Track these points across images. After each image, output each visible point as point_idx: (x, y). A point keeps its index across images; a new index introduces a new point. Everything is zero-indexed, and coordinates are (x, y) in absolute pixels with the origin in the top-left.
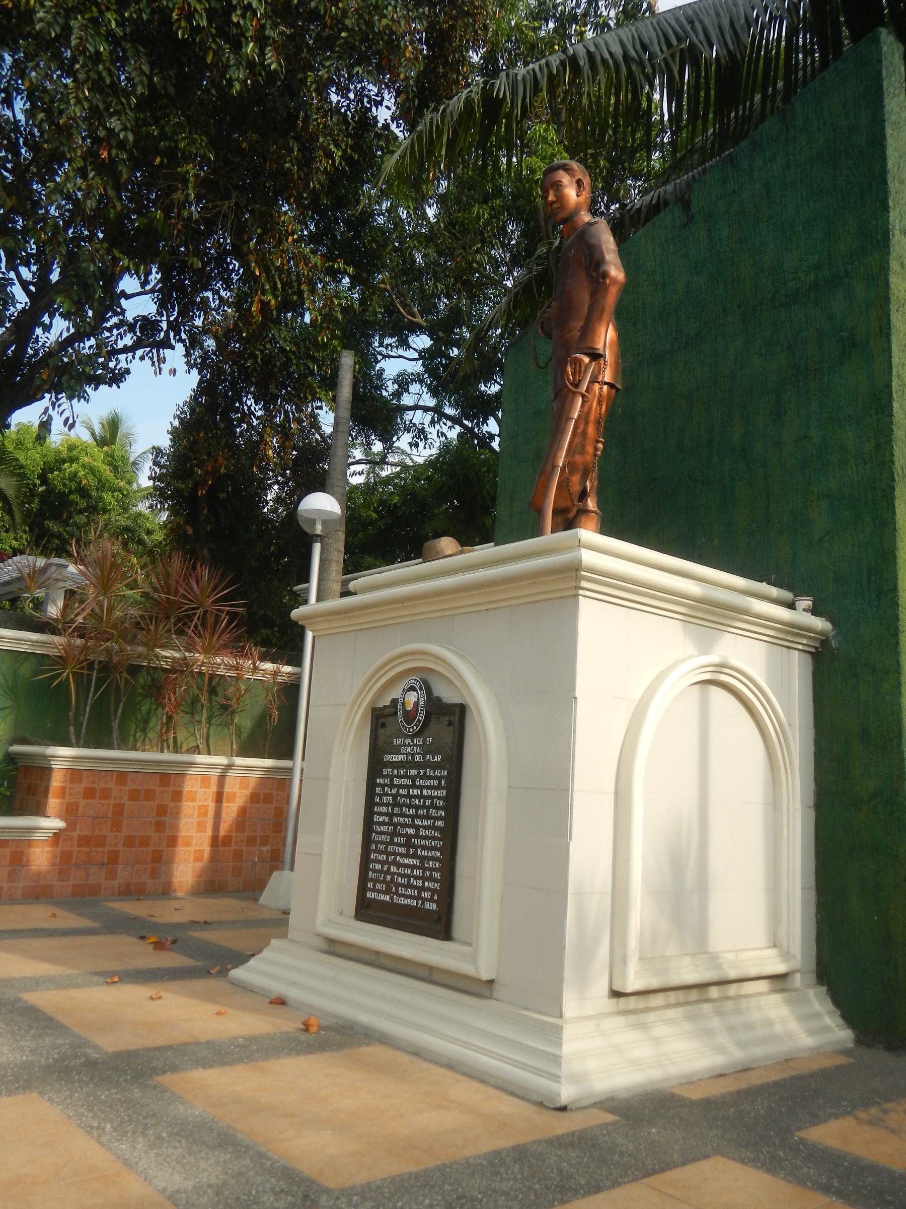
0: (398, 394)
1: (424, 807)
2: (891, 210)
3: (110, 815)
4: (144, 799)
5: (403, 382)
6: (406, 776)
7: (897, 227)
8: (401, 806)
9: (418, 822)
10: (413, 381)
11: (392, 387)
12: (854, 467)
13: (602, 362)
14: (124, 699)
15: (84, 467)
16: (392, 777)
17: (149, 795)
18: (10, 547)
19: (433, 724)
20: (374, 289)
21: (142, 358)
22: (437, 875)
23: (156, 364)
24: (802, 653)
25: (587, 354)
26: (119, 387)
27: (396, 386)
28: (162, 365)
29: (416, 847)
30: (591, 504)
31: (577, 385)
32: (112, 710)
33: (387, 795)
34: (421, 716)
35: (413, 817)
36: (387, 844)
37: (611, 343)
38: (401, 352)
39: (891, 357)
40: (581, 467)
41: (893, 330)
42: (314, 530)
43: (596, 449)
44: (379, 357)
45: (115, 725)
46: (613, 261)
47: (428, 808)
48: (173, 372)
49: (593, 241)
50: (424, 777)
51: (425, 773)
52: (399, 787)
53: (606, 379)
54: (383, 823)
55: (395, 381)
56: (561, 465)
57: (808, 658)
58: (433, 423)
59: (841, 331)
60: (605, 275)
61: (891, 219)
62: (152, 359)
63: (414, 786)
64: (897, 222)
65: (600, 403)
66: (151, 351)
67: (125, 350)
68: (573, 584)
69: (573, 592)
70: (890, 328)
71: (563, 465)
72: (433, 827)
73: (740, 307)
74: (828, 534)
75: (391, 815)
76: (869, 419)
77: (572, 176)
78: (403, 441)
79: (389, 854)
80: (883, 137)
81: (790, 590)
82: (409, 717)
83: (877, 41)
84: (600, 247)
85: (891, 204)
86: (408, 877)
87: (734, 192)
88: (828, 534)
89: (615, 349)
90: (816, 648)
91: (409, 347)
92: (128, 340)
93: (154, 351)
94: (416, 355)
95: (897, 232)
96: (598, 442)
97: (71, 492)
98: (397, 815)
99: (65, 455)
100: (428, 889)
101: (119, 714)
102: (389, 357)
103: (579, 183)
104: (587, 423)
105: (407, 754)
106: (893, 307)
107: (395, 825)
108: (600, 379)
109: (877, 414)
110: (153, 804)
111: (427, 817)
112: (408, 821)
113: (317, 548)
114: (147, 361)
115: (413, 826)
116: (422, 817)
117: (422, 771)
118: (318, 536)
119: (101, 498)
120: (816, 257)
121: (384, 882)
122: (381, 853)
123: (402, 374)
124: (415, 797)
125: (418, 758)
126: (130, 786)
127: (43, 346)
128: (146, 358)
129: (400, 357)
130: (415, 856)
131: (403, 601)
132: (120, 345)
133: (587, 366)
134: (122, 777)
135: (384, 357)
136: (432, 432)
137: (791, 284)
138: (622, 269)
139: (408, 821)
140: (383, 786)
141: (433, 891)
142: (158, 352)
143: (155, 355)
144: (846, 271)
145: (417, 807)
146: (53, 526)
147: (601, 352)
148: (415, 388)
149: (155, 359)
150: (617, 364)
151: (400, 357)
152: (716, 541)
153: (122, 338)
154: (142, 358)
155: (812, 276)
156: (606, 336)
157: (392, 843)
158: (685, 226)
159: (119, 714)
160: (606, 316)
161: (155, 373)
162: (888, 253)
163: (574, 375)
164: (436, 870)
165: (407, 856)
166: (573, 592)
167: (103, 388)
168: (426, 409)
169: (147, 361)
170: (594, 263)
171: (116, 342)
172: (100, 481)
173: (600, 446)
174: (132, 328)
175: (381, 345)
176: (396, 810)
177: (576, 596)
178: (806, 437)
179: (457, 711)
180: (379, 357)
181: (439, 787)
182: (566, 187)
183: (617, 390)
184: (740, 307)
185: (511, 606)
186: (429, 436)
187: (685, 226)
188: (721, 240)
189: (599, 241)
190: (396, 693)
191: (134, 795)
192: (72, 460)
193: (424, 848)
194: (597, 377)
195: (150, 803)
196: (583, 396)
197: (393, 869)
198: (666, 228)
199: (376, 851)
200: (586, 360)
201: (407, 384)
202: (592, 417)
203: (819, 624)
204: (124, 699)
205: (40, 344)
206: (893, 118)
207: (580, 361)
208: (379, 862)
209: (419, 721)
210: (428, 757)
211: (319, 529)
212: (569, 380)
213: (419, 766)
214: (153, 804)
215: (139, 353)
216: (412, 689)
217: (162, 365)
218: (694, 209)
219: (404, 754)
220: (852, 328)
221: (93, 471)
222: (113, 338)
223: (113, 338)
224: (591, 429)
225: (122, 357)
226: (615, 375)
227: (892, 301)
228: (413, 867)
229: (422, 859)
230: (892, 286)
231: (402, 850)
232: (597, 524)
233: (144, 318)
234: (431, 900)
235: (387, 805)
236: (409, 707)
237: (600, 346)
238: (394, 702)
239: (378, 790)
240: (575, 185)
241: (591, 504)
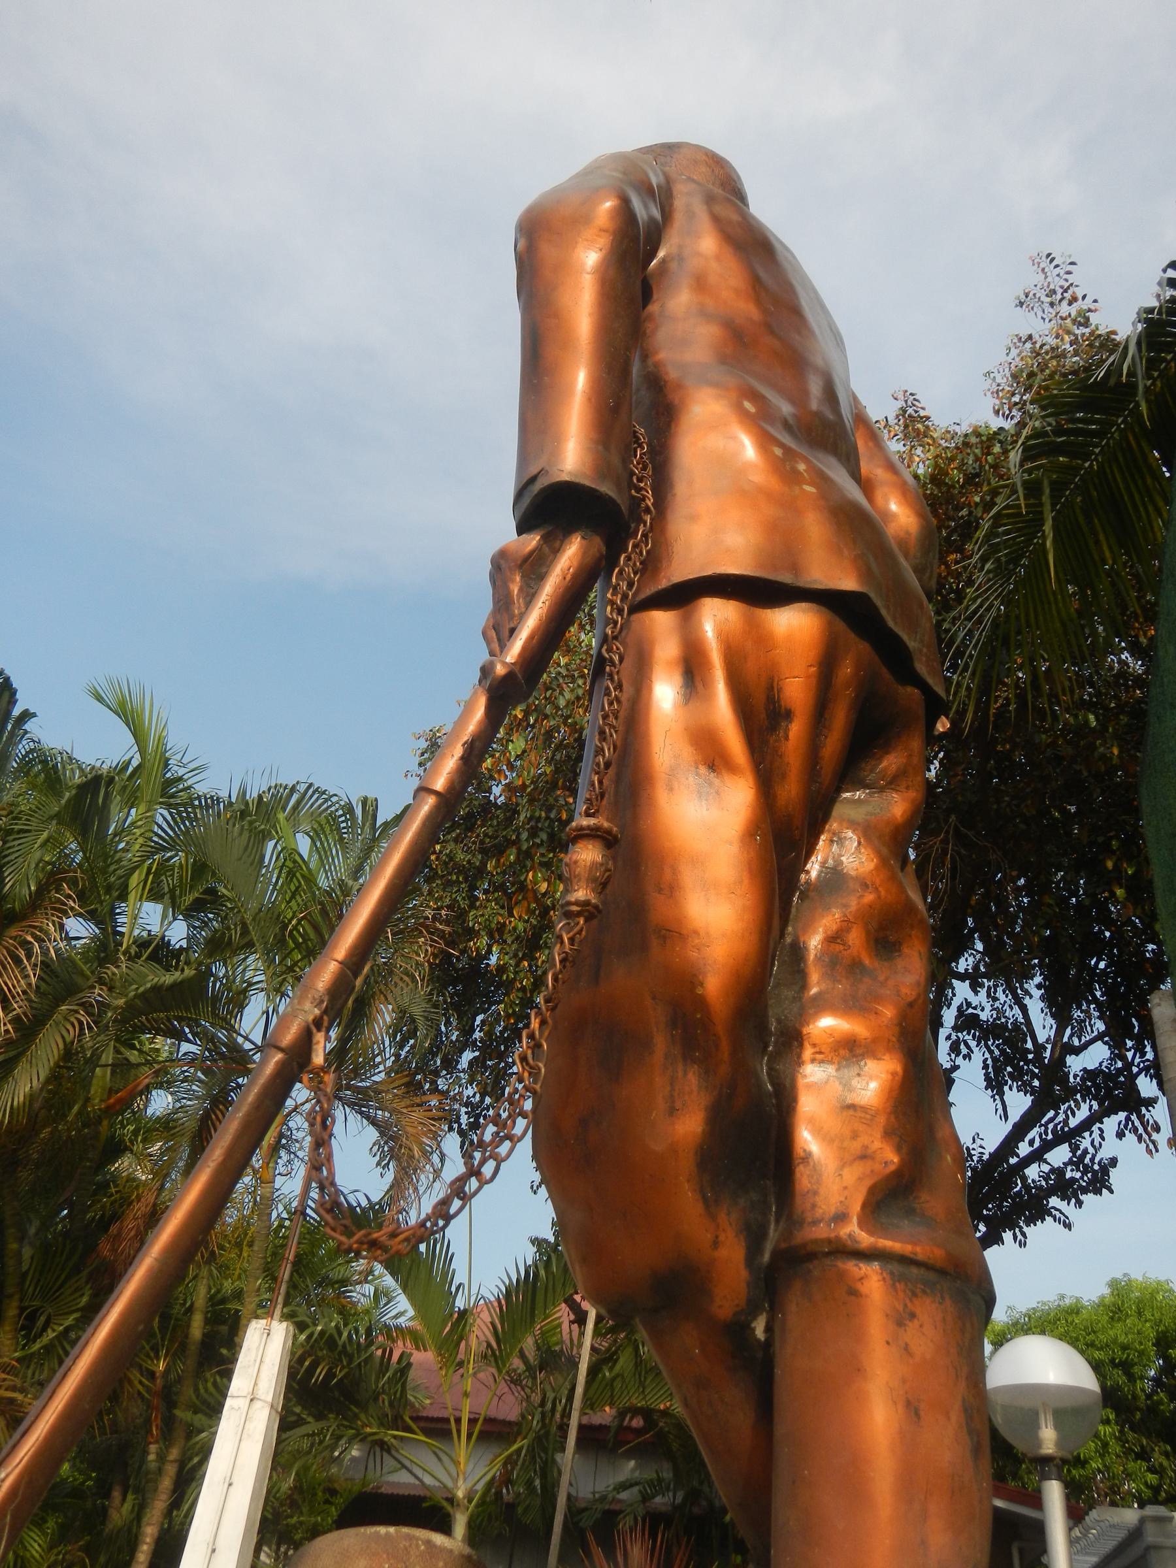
18: (1146, 1484)
21: (1120, 1135)
23: (1144, 1135)
26: (1112, 1192)
28: (1155, 1136)
40: (656, 1016)
42: (1038, 1443)
62: (1135, 1130)
66: (1128, 1119)
67: (1086, 1125)
92: (1083, 1113)
93: (1134, 1117)
114: (1130, 1137)
118: (1047, 1460)
127: (980, 1160)
128: (1127, 1132)
132: (1073, 1122)
142: (1141, 1117)
143: (1137, 1123)
149: (1141, 1130)
153: (1074, 1114)
154: (1120, 1135)
161: (1149, 1152)
167: (1088, 1198)
169: (1130, 1137)
171: (1066, 1122)
205: (975, 1158)
211: (1048, 1438)
215: (1111, 1124)
217: (1155, 1136)
222: (1061, 1117)
223: (1061, 1117)
225: (1085, 1143)
232: (901, 1319)
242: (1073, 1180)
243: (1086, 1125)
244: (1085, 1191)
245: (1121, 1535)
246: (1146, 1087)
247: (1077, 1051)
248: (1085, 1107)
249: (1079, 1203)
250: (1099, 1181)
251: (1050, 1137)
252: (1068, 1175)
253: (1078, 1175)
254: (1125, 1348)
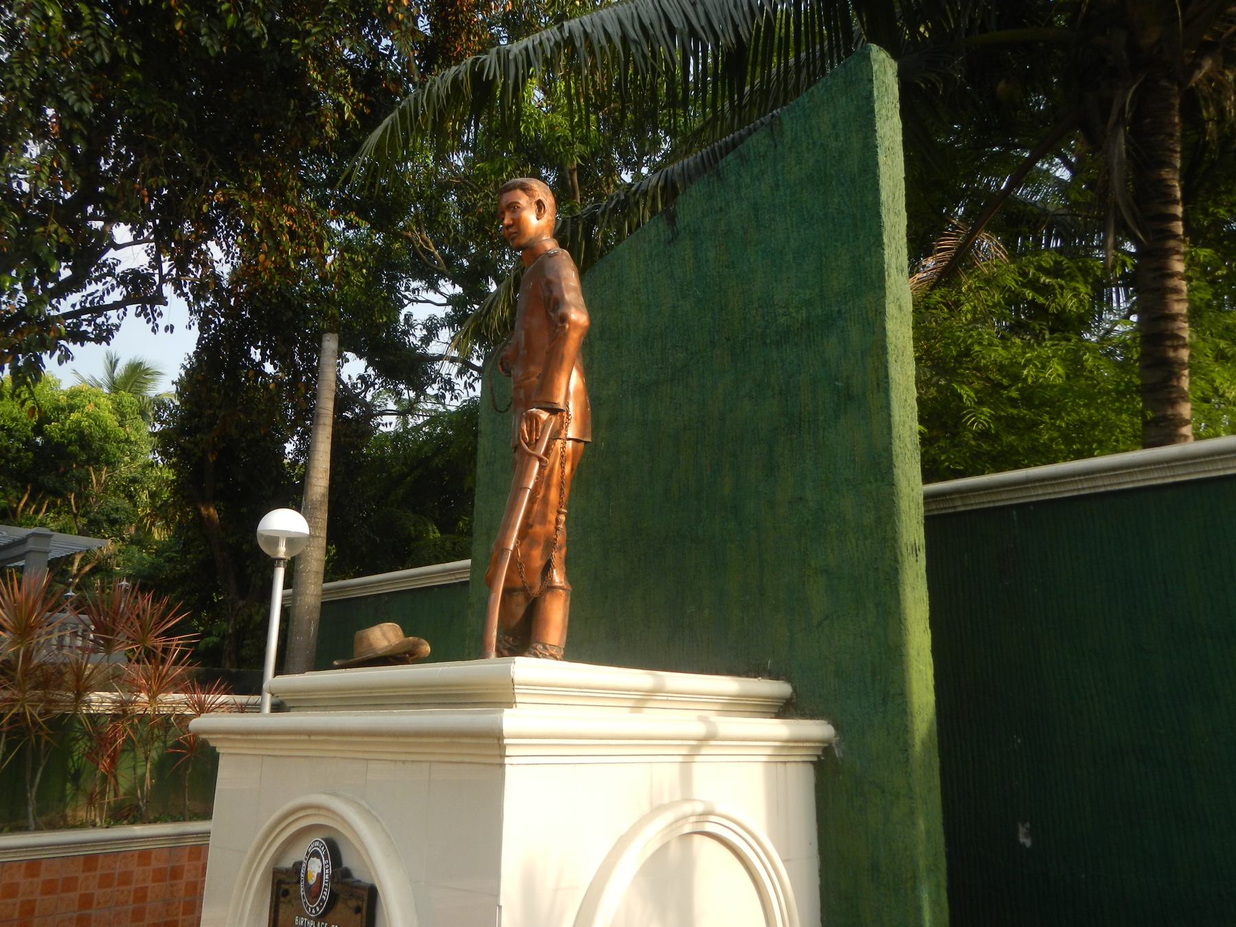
0: (426, 340)
2: (886, 247)
3: (16, 915)
4: (63, 891)
5: (432, 328)
7: (894, 266)
10: (442, 326)
11: (420, 333)
12: (853, 541)
13: (565, 414)
14: (44, 762)
15: (88, 415)
17: (69, 884)
19: (340, 906)
20: (397, 236)
24: (801, 765)
25: (546, 410)
27: (425, 332)
30: (558, 578)
31: (534, 444)
32: (28, 777)
34: (325, 895)
37: (576, 392)
38: (431, 295)
39: (890, 416)
40: (542, 540)
41: (893, 386)
42: (277, 552)
43: (557, 521)
44: (406, 302)
45: (32, 795)
46: (573, 301)
48: (169, 328)
49: (551, 277)
53: (571, 434)
55: (425, 326)
56: (511, 547)
57: (811, 768)
58: (460, 373)
59: (837, 380)
60: (564, 319)
61: (886, 257)
64: (894, 260)
65: (562, 465)
68: (497, 752)
69: (498, 760)
70: (888, 382)
71: (515, 548)
73: (728, 340)
74: (827, 617)
76: (868, 486)
77: (531, 196)
78: (432, 390)
80: (877, 164)
81: (788, 680)
82: (313, 892)
83: (867, 57)
84: (560, 284)
85: (885, 240)
87: (721, 209)
88: (827, 617)
89: (582, 398)
90: (818, 756)
91: (436, 290)
92: (117, 295)
94: (444, 301)
95: (893, 271)
96: (559, 513)
97: (70, 443)
99: (63, 401)
101: (37, 780)
102: (418, 301)
103: (540, 204)
104: (548, 487)
106: (891, 359)
108: (562, 436)
109: (876, 480)
110: (75, 895)
113: (280, 574)
119: (103, 449)
120: (808, 292)
123: (430, 319)
126: (44, 876)
129: (428, 301)
131: (310, 734)
132: (108, 300)
133: (546, 423)
134: (33, 867)
135: (411, 301)
136: (459, 383)
137: (782, 320)
138: (585, 310)
144: (839, 311)
146: (50, 480)
147: (562, 406)
148: (445, 334)
150: (584, 415)
151: (428, 301)
152: (706, 612)
155: (804, 313)
156: (571, 385)
158: (670, 242)
159: (37, 780)
160: (566, 365)
162: (884, 296)
163: (530, 433)
166: (498, 760)
167: (90, 345)
168: (453, 360)
170: (552, 305)
171: (102, 298)
172: (104, 431)
173: (563, 518)
174: (123, 280)
175: (407, 289)
177: (502, 765)
178: (801, 499)
179: (365, 894)
180: (406, 302)
182: (524, 209)
183: (586, 443)
184: (728, 340)
185: (431, 762)
186: (456, 387)
187: (670, 242)
188: (707, 261)
189: (559, 277)
190: (298, 854)
191: (49, 888)
192: (72, 409)
194: (559, 432)
195: (71, 895)
196: (540, 460)
198: (650, 241)
200: (544, 415)
201: (436, 329)
202: (555, 479)
203: (818, 729)
204: (44, 762)
206: (887, 143)
207: (536, 418)
209: (322, 900)
211: (282, 551)
212: (524, 439)
214: (75, 895)
215: (132, 309)
216: (315, 854)
217: (158, 320)
218: (680, 224)
220: (848, 377)
221: (96, 418)
224: (554, 495)
226: (583, 431)
227: (890, 350)
230: (889, 334)
233: (135, 272)
236: (312, 880)
237: (560, 401)
238: (298, 865)
240: (535, 207)
241: (558, 578)
242: (85, 331)
243: (116, 306)
244: (90, 340)
245: (7, 541)
246: (168, 290)
247: (118, 247)
248: (118, 291)
249: (82, 345)
250: (104, 335)
251: (88, 305)
252: (84, 328)
253: (90, 329)
254: (14, 420)
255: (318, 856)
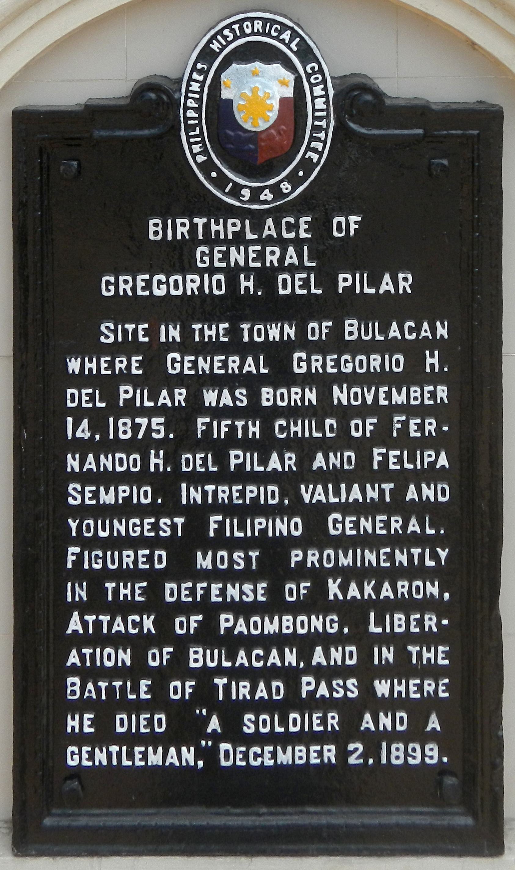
1: (343, 440)
6: (236, 346)
8: (219, 449)
9: (313, 494)
16: (154, 354)
22: (439, 655)
29: (319, 577)
33: (131, 409)
35: (288, 482)
36: (155, 580)
47: (363, 447)
50: (336, 343)
51: (337, 331)
52: (197, 383)
54: (126, 509)
63: (281, 376)
72: (398, 506)
75: (166, 485)
79: (166, 614)
86: (291, 676)
98: (197, 479)
100: (391, 704)
105: (233, 274)
107: (197, 515)
111: (364, 473)
112: (272, 493)
115: (294, 507)
116: (333, 477)
117: (318, 329)
121: (159, 700)
122: (123, 608)
124: (293, 412)
125: (288, 286)
130: (317, 602)
139: (272, 493)
140: (108, 385)
141: (419, 710)
145: (305, 448)
157: (182, 567)
164: (426, 639)
165: (275, 605)
176: (194, 461)
181: (414, 374)
193: (347, 575)
197: (197, 657)
199: (96, 602)
208: (119, 641)
210: (344, 280)
213: (296, 310)
219: (212, 270)
228: (305, 644)
229: (353, 613)
231: (254, 592)
234: (417, 733)
235: (142, 445)
239: (78, 397)
255: (269, 54)
